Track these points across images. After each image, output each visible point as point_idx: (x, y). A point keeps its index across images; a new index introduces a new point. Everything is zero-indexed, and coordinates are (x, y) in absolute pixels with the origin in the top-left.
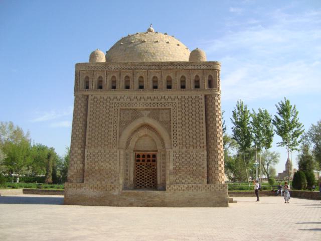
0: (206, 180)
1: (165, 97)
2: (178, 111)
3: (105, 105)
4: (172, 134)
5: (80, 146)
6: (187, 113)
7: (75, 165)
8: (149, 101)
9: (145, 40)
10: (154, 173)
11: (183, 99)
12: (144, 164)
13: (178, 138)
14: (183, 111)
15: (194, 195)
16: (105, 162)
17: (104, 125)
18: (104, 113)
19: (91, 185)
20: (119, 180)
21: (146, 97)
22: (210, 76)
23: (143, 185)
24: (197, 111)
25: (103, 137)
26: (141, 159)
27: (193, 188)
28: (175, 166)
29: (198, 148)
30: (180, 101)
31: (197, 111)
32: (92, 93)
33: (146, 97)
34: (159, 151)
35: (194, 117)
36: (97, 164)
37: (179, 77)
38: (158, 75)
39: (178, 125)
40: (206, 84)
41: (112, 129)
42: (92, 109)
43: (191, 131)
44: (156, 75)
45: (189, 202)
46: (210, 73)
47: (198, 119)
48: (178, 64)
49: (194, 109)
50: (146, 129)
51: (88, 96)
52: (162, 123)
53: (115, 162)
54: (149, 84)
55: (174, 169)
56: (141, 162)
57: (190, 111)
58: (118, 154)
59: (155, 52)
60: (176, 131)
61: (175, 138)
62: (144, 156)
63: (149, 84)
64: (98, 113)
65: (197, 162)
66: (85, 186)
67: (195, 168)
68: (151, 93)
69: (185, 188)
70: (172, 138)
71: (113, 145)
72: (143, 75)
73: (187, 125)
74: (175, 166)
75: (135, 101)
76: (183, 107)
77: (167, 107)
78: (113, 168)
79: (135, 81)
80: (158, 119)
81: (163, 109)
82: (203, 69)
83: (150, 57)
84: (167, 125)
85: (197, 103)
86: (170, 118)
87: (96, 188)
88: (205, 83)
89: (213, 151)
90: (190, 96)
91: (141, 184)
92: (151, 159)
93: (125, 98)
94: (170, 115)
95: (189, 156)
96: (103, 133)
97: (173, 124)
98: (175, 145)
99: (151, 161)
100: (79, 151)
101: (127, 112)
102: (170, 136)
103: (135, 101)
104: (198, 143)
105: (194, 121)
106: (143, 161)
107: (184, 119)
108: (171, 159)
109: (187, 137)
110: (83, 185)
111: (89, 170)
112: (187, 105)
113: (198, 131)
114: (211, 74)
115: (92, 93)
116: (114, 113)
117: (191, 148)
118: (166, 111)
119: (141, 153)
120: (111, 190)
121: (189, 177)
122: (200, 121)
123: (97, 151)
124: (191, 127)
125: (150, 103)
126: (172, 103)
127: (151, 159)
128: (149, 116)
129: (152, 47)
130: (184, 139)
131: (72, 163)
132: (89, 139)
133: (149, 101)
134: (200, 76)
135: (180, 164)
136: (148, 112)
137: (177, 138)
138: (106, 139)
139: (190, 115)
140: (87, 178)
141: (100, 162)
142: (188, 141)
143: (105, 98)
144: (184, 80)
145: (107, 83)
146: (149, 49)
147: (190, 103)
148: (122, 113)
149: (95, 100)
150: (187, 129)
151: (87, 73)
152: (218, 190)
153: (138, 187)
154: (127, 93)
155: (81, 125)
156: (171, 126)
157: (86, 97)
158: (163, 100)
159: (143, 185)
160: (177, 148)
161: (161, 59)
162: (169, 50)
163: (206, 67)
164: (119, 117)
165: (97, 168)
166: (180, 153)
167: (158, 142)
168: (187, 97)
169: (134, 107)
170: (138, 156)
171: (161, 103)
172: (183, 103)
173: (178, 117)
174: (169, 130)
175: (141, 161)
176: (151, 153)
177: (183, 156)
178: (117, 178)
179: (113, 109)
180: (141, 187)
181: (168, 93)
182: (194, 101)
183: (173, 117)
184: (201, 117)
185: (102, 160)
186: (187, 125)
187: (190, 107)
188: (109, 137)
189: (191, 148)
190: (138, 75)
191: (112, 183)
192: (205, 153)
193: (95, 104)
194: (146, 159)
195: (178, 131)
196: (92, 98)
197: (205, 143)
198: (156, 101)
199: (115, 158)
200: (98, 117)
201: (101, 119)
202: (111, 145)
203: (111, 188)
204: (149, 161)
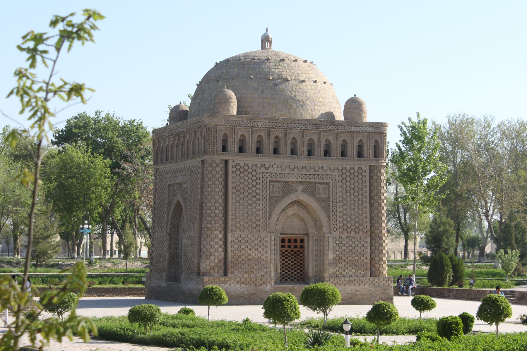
0: (370, 273)
1: (322, 167)
2: (338, 186)
3: (250, 176)
4: (331, 216)
5: (220, 229)
7: (217, 254)
8: (304, 172)
9: (289, 79)
10: (302, 262)
11: (344, 171)
12: (289, 250)
13: (338, 220)
14: (344, 186)
15: (356, 290)
16: (253, 250)
17: (250, 202)
18: (250, 186)
19: (238, 279)
20: (271, 272)
21: (300, 167)
22: (376, 141)
23: (289, 278)
24: (360, 187)
25: (249, 218)
26: (287, 244)
27: (356, 282)
29: (361, 232)
30: (341, 173)
31: (360, 187)
32: (234, 158)
33: (300, 167)
34: (311, 235)
36: (243, 252)
37: (340, 141)
38: (315, 138)
39: (338, 204)
40: (372, 152)
41: (261, 207)
42: (234, 180)
43: (353, 212)
44: (313, 138)
45: (350, 298)
46: (377, 137)
47: (360, 197)
48: (341, 124)
49: (356, 184)
50: (296, 207)
51: (226, 162)
52: (320, 200)
53: (265, 249)
54: (303, 149)
55: (334, 258)
57: (352, 186)
58: (268, 239)
59: (304, 99)
60: (336, 211)
61: (335, 221)
62: (289, 241)
63: (303, 149)
64: (242, 186)
65: (359, 250)
66: (230, 281)
67: (357, 258)
68: (307, 162)
69: (346, 282)
70: (332, 220)
71: (262, 228)
72: (296, 136)
73: (348, 204)
74: (334, 256)
75: (287, 171)
76: (344, 181)
77: (325, 180)
78: (263, 257)
79: (288, 144)
80: (312, 194)
81: (320, 183)
82: (369, 133)
83: (300, 107)
84: (325, 203)
85: (360, 177)
86: (329, 195)
87: (243, 282)
88: (369, 151)
89: (376, 238)
90: (353, 167)
91: (286, 276)
92: (299, 244)
93: (275, 166)
94: (329, 191)
96: (250, 212)
97: (333, 202)
98: (335, 229)
99: (299, 246)
100: (220, 236)
101: (278, 185)
102: (329, 217)
103: (287, 171)
104: (361, 227)
105: (356, 199)
106: (289, 247)
107: (345, 196)
108: (331, 247)
109: (349, 219)
110: (227, 279)
111: (234, 259)
112: (348, 179)
113: (360, 212)
114: (377, 139)
115: (234, 158)
116: (263, 186)
117: (353, 233)
118: (325, 186)
119: (287, 237)
120: (261, 285)
121: (350, 268)
122: (363, 199)
123: (243, 236)
124: (353, 207)
125: (306, 175)
126: (331, 175)
127: (299, 244)
128: (303, 191)
129: (299, 90)
130: (345, 222)
131: (212, 250)
132: (232, 220)
133: (304, 172)
134: (364, 140)
135: (341, 253)
136: (302, 186)
137: (336, 220)
138: (254, 220)
140: (232, 270)
141: (248, 249)
142: (349, 225)
143: (250, 165)
144: (344, 144)
145: (251, 144)
146: (297, 93)
148: (271, 188)
149: (238, 167)
150: (349, 210)
151: (226, 128)
152: (382, 284)
154: (277, 160)
155: (220, 201)
156: (329, 205)
157: (224, 162)
158: (321, 170)
159: (289, 278)
160: (337, 232)
161: (311, 110)
162: (319, 95)
164: (268, 191)
165: (243, 257)
166: (341, 240)
167: (310, 223)
168: (348, 168)
169: (286, 180)
170: (283, 241)
171: (318, 175)
172: (344, 176)
173: (338, 194)
174: (327, 209)
175: (286, 246)
176: (299, 237)
177: (344, 242)
178: (268, 270)
179: (261, 181)
181: (326, 163)
183: (333, 193)
184: (364, 194)
185: (250, 247)
186: (348, 204)
187: (352, 181)
188: (257, 218)
189: (353, 233)
190: (291, 136)
191: (263, 276)
192: (369, 240)
193: (238, 173)
194: (292, 244)
195: (338, 211)
196: (234, 164)
197: (369, 227)
198: (312, 172)
199: (265, 244)
200: (242, 191)
201: (246, 194)
202: (261, 229)
203: (262, 282)
204: (295, 247)
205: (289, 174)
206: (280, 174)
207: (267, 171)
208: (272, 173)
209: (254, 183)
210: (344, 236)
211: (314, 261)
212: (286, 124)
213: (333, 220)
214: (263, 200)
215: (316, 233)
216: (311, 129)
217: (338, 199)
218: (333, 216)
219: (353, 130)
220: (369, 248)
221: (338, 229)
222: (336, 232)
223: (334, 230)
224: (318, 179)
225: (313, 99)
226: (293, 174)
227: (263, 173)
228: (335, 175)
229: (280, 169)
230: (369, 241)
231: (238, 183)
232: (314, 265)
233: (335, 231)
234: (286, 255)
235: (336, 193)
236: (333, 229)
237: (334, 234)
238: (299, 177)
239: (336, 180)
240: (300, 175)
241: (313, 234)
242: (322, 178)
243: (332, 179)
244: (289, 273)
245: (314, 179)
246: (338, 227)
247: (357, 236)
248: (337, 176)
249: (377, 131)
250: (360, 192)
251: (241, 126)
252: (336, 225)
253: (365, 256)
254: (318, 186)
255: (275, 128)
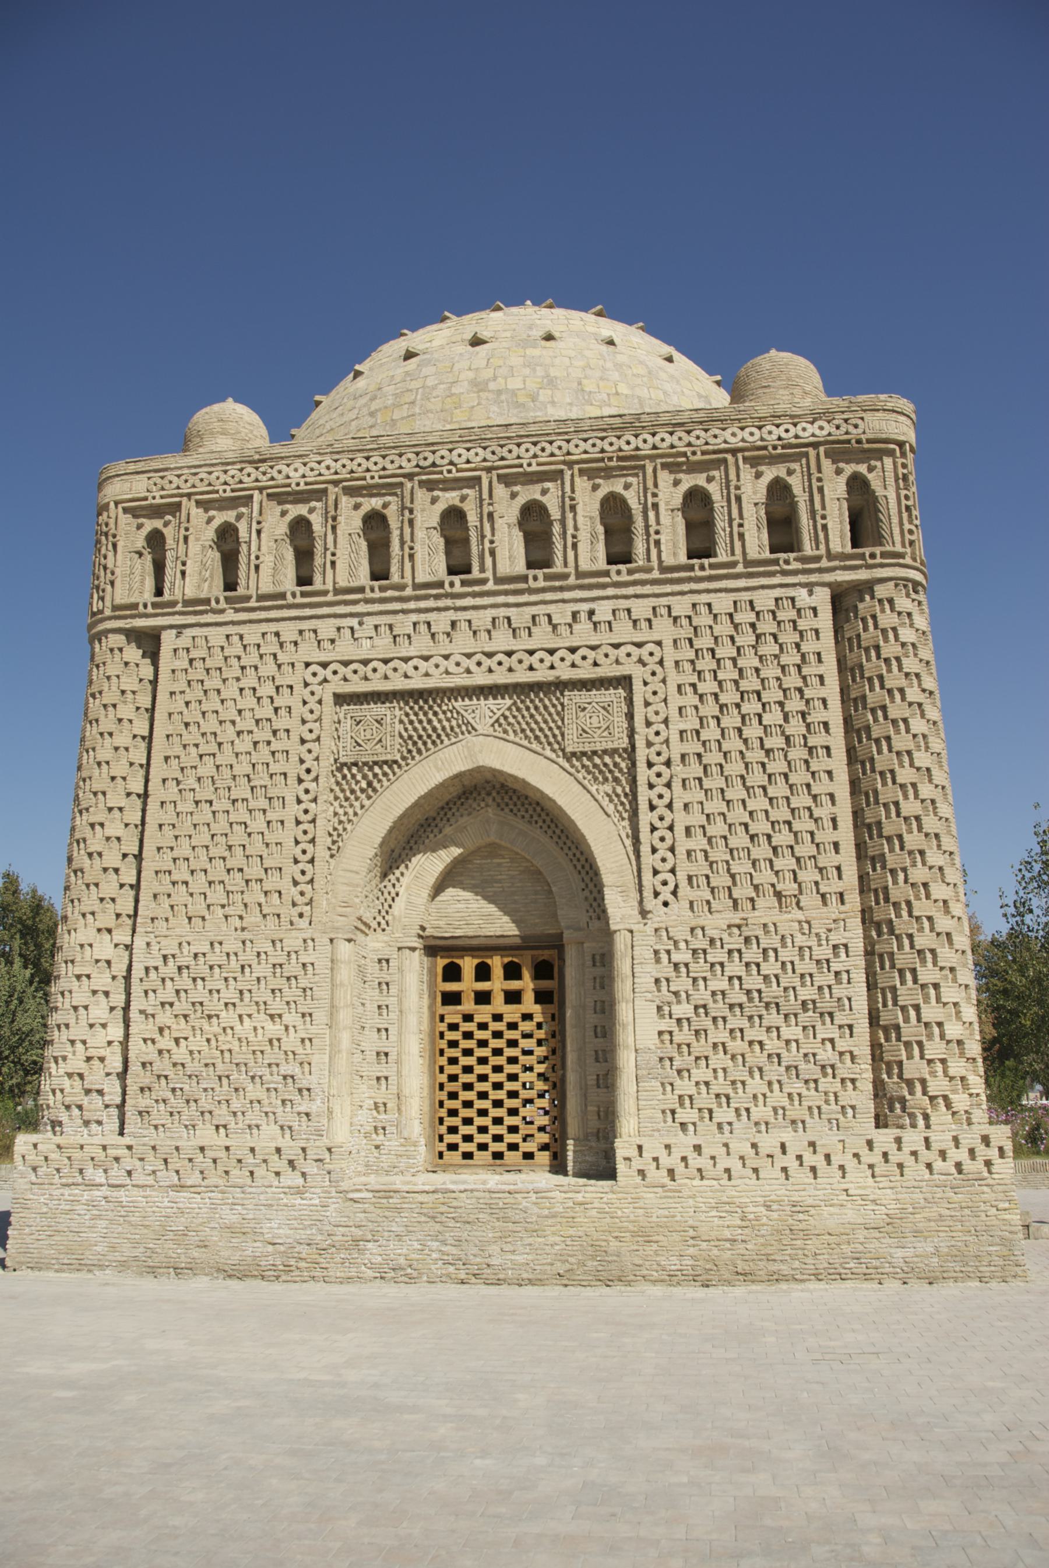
2: (672, 688)
6: (729, 697)
11: (704, 619)
12: (483, 1013)
14: (708, 686)
17: (242, 791)
18: (247, 723)
23: (483, 1147)
26: (468, 984)
28: (666, 1024)
30: (687, 632)
31: (792, 681)
35: (773, 717)
47: (796, 727)
50: (491, 812)
56: (468, 1005)
60: (670, 806)
75: (422, 644)
76: (706, 664)
77: (608, 670)
78: (291, 1042)
86: (632, 733)
94: (630, 716)
95: (752, 954)
104: (809, 875)
105: (775, 742)
107: (711, 733)
108: (645, 981)
109: (740, 840)
124: (757, 778)
125: (509, 654)
126: (639, 645)
130: (719, 854)
133: (502, 640)
137: (672, 849)
139: (752, 707)
147: (746, 639)
153: (455, 1157)
158: (584, 626)
159: (483, 1147)
160: (679, 909)
163: (828, 428)
166: (701, 943)
169: (417, 683)
170: (452, 973)
171: (573, 650)
172: (704, 642)
177: (717, 955)
180: (468, 1156)
182: (767, 626)
184: (817, 716)
192: (854, 935)
194: (497, 984)
195: (678, 805)
198: (542, 637)
205: (426, 659)
206: (386, 661)
207: (323, 657)
208: (346, 664)
209: (267, 711)
210: (716, 923)
211: (590, 1060)
212: (412, 456)
213: (654, 850)
214: (300, 781)
215: (596, 924)
216: (525, 462)
217: (677, 749)
218: (654, 829)
219: (735, 442)
220: (860, 977)
221: (684, 890)
222: (674, 905)
223: (661, 898)
224: (573, 665)
225: (580, 383)
226: (446, 657)
227: (307, 665)
228: (659, 643)
229: (384, 640)
230: (858, 945)
231: (193, 715)
232: (591, 1080)
233: (666, 904)
234: (468, 1035)
235: (666, 721)
236: (656, 894)
237: (659, 916)
238: (474, 668)
239: (661, 662)
240: (478, 657)
241: (580, 929)
242: (590, 661)
243: (641, 661)
244: (479, 1121)
245: (552, 667)
246: (683, 883)
247: (788, 920)
248: (668, 643)
249: (854, 431)
250: (795, 705)
251: (217, 492)
252: (673, 871)
253: (840, 1018)
254: (574, 698)
255: (364, 479)
